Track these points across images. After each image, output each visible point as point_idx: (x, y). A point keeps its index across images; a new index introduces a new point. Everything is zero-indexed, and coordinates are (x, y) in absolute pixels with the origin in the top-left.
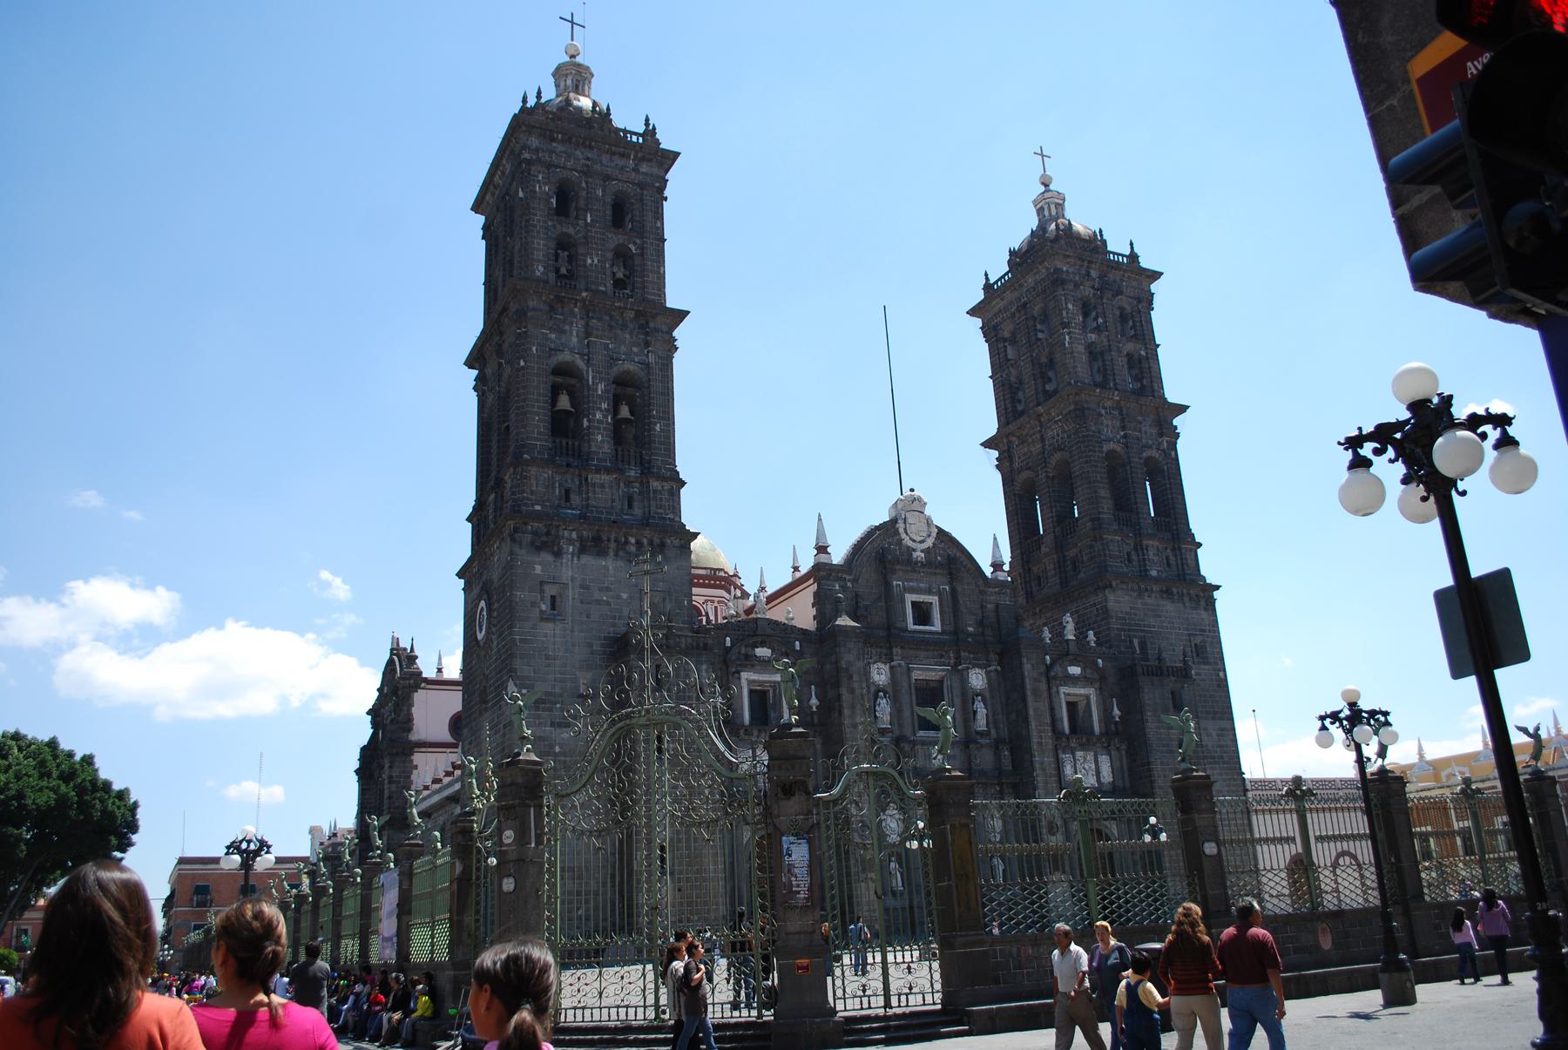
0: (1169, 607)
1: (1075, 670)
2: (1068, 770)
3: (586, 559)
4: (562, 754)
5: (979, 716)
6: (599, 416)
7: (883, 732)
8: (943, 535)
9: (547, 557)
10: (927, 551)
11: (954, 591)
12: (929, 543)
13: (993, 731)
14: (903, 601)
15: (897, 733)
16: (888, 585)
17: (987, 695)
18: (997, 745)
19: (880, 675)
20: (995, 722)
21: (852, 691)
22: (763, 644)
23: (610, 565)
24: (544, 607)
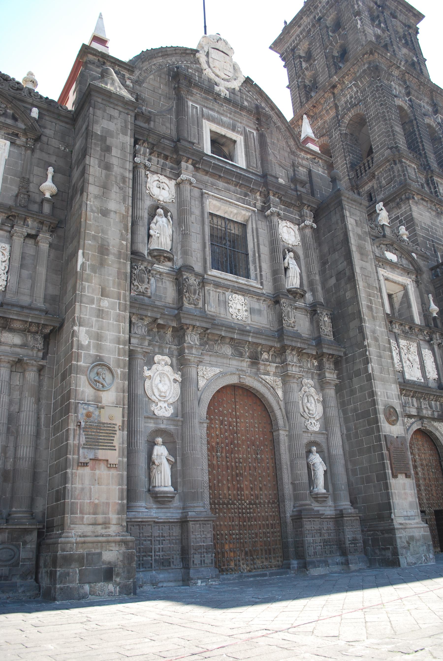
1: (391, 256)
5: (291, 273)
10: (232, 91)
12: (236, 85)
13: (309, 296)
14: (199, 126)
15: (179, 262)
17: (301, 253)
18: (313, 311)
19: (160, 188)
20: (311, 284)
21: (107, 167)
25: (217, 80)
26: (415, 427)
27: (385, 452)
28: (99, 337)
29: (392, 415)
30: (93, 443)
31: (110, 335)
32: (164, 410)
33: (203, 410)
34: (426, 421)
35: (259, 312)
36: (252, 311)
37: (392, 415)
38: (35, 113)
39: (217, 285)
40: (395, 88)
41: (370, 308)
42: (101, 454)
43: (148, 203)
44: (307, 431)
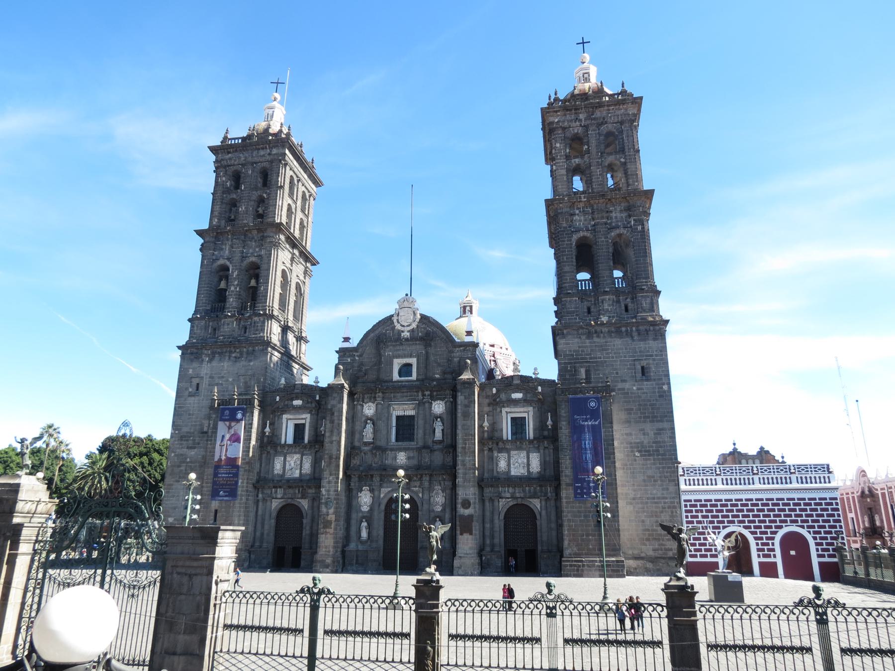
0: (618, 342)
2: (502, 464)
3: (215, 363)
4: (191, 462)
6: (232, 288)
7: (366, 444)
8: (424, 318)
9: (195, 365)
10: (412, 331)
11: (427, 353)
12: (414, 325)
14: (391, 364)
16: (379, 355)
22: (297, 399)
23: (226, 364)
24: (190, 390)
25: (402, 329)
26: (511, 504)
27: (458, 523)
28: (328, 491)
29: (466, 504)
30: (324, 528)
31: (332, 489)
32: (365, 508)
33: (383, 507)
34: (519, 500)
35: (413, 458)
36: (409, 458)
37: (466, 504)
38: (317, 398)
39: (392, 450)
40: (580, 221)
41: (464, 448)
42: (328, 530)
43: (364, 419)
44: (433, 511)
